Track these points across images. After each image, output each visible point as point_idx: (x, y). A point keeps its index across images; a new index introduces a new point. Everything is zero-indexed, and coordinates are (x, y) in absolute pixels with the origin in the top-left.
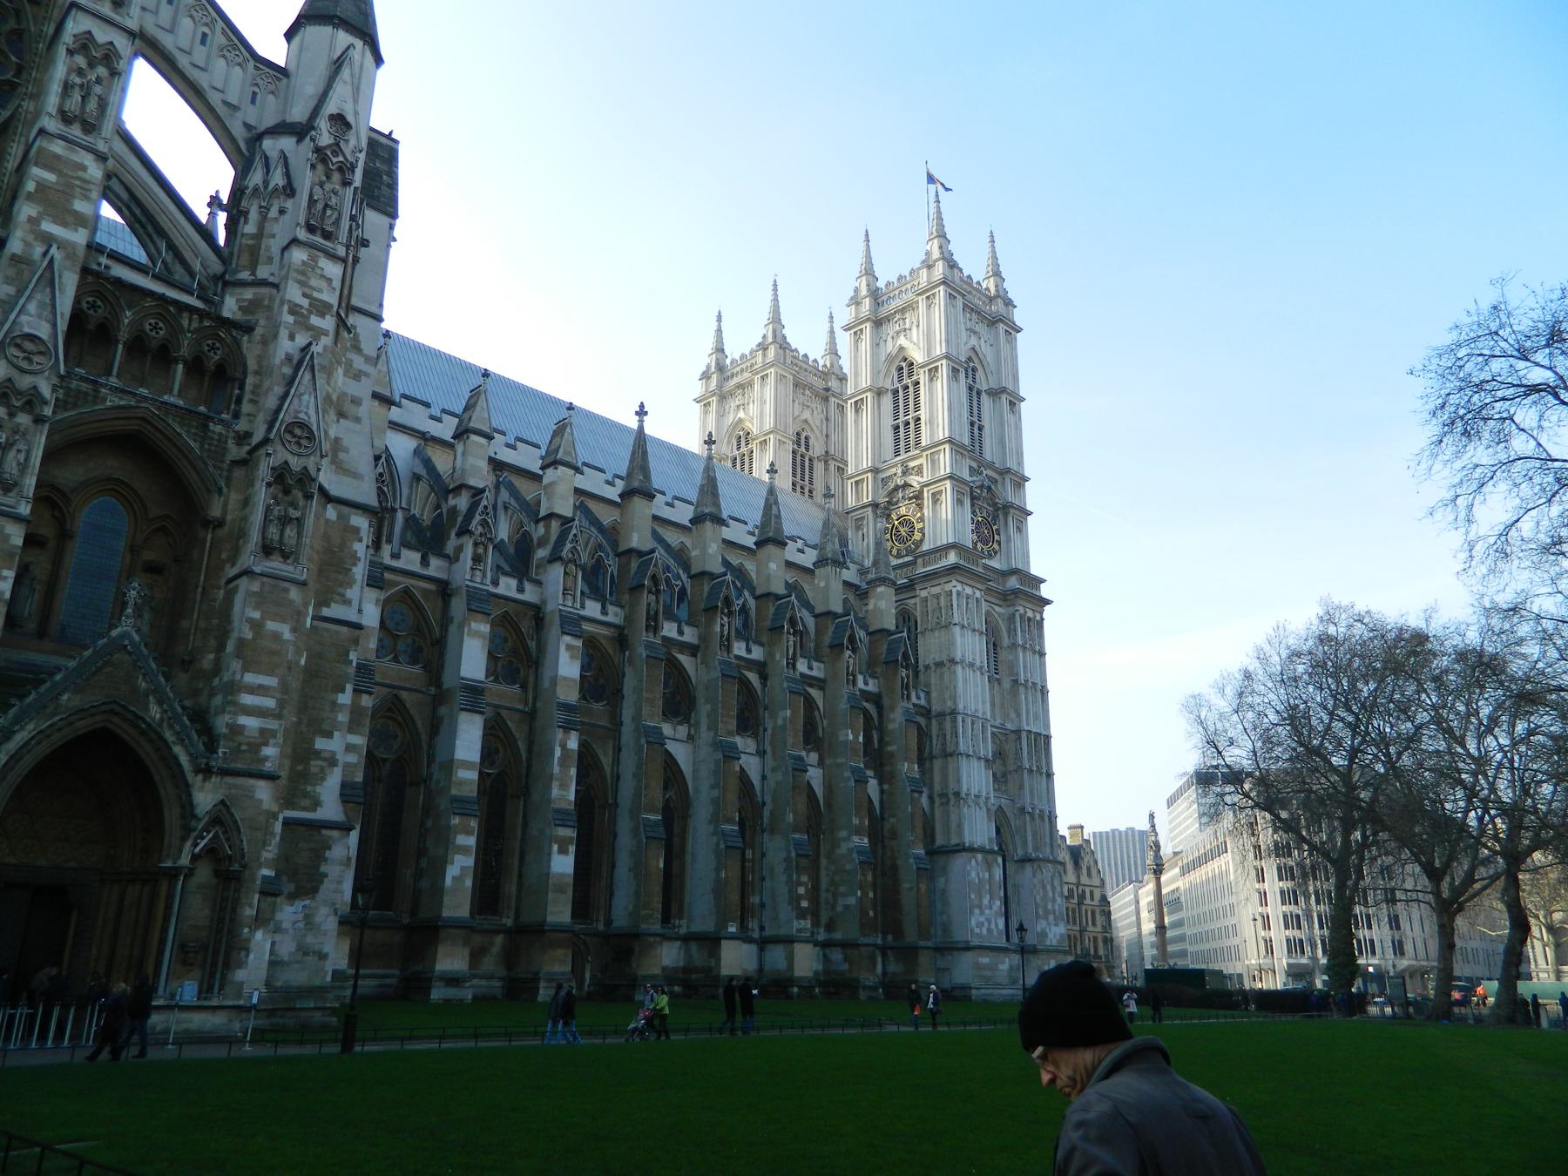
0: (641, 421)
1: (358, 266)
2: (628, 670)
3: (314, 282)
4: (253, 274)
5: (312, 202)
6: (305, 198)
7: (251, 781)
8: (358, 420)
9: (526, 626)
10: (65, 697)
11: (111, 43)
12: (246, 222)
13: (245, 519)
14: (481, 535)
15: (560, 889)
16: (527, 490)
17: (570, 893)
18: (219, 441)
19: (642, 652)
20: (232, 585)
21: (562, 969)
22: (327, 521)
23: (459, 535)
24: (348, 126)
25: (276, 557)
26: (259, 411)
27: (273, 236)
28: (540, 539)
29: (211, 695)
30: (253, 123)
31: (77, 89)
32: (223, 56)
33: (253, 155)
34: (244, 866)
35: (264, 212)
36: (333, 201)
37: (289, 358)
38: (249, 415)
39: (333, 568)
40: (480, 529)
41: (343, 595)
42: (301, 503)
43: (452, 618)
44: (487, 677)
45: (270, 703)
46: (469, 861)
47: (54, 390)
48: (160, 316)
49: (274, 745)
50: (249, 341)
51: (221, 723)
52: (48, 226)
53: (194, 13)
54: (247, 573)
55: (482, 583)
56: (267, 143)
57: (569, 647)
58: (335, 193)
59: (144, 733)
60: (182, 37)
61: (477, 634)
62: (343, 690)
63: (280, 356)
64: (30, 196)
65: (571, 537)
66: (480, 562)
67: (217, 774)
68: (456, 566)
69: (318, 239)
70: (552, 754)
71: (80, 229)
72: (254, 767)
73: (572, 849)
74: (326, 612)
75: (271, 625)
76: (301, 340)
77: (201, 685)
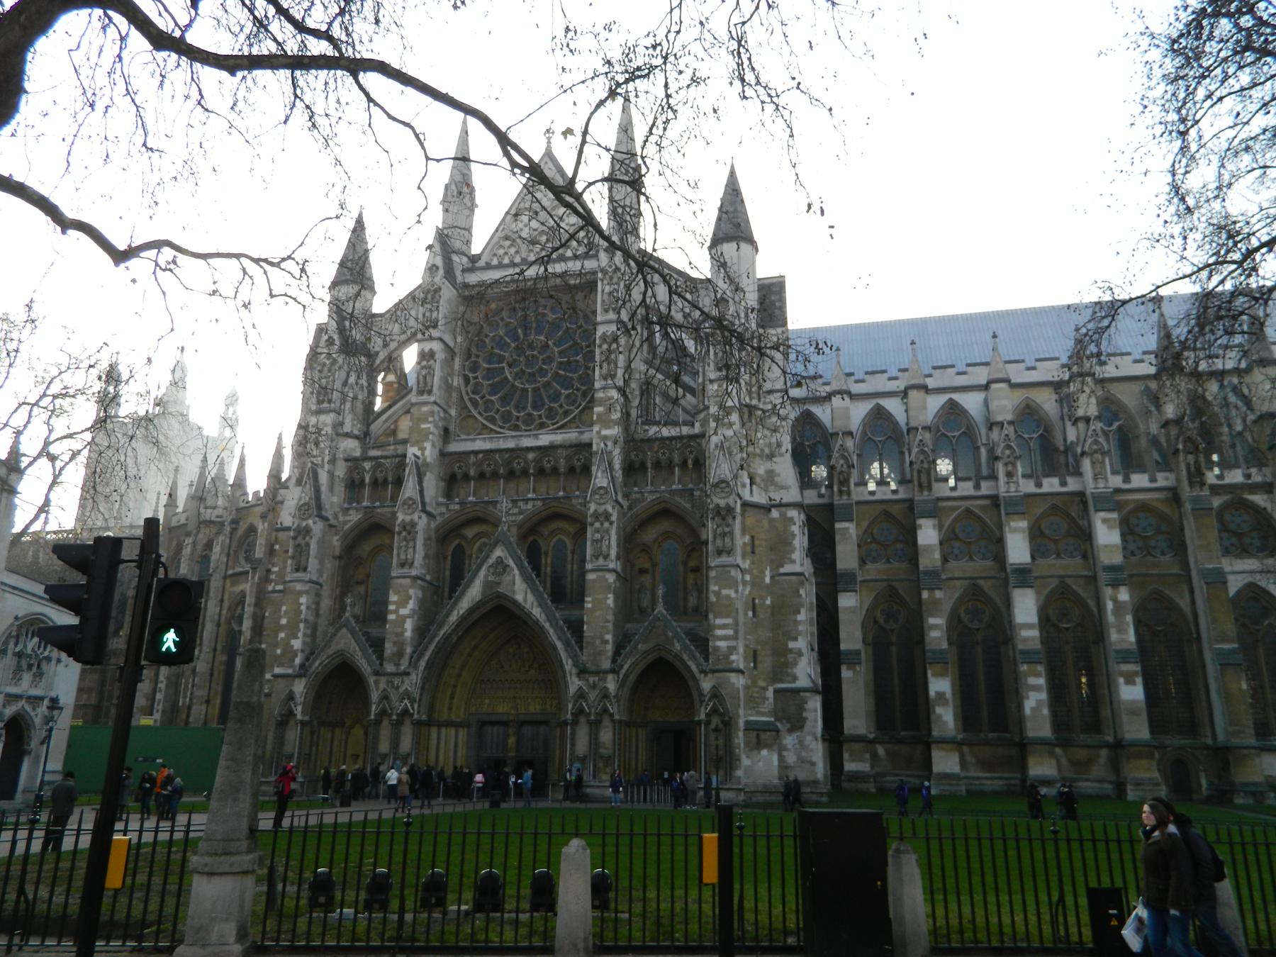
2: (1185, 523)
7: (728, 674)
14: (1009, 457)
15: (1134, 712)
17: (1144, 715)
19: (1188, 506)
21: (1148, 775)
34: (731, 718)
37: (716, 445)
40: (1008, 452)
41: (790, 559)
45: (730, 632)
46: (1043, 696)
49: (738, 654)
52: (605, 432)
55: (1017, 491)
57: (1104, 521)
61: (1016, 530)
62: (799, 613)
63: (712, 446)
70: (1105, 608)
73: (1139, 680)
74: (782, 570)
75: (724, 592)
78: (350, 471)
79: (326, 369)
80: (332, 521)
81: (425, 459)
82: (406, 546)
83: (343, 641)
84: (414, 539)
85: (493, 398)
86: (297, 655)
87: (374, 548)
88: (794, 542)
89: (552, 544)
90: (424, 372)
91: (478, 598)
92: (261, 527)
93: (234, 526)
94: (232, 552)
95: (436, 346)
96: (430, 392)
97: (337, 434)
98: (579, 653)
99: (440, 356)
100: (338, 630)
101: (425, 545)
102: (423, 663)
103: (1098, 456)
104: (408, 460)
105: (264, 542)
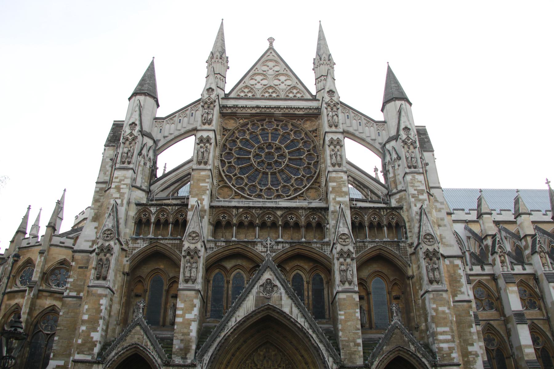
0: (549, 186)
1: (427, 173)
3: (416, 184)
4: (397, 189)
5: (407, 158)
6: (405, 158)
8: (445, 226)
9: (532, 283)
10: (384, 348)
11: (338, 138)
12: (389, 174)
13: (420, 273)
14: (501, 252)
16: (512, 228)
18: (404, 249)
20: (423, 297)
22: (447, 265)
23: (492, 255)
24: (409, 129)
25: (435, 284)
26: (413, 234)
27: (399, 174)
28: (524, 247)
29: (428, 338)
30: (381, 142)
31: (333, 155)
32: (367, 126)
33: (384, 152)
35: (393, 167)
36: (413, 156)
37: (417, 213)
38: (410, 237)
39: (454, 280)
40: (500, 250)
41: (460, 291)
42: (437, 262)
43: (501, 288)
44: (523, 308)
45: (449, 337)
47: (354, 248)
48: (375, 214)
50: (403, 212)
51: (435, 347)
52: (338, 199)
53: (355, 118)
54: (427, 292)
56: (388, 146)
58: (413, 152)
59: (411, 356)
60: (354, 126)
61: (513, 292)
62: (472, 327)
63: (414, 213)
64: (331, 192)
65: (537, 242)
66: (504, 263)
67: (439, 367)
68: (495, 267)
69: (413, 170)
71: (346, 196)
72: (451, 362)
74: (457, 299)
75: (440, 309)
76: (419, 205)
77: (424, 335)
78: (139, 212)
79: (128, 143)
80: (124, 247)
81: (203, 207)
82: (190, 267)
83: (136, 336)
84: (196, 262)
85: (243, 176)
86: (96, 345)
87: (151, 271)
88: (462, 280)
89: (292, 276)
90: (202, 150)
91: (254, 309)
92: (38, 260)
93: (16, 259)
94: (11, 276)
95: (212, 135)
96: (206, 163)
97: (133, 186)
98: (337, 353)
99: (213, 141)
100: (133, 327)
101: (203, 268)
102: (207, 358)
103: (542, 254)
104: (189, 207)
105: (40, 270)
